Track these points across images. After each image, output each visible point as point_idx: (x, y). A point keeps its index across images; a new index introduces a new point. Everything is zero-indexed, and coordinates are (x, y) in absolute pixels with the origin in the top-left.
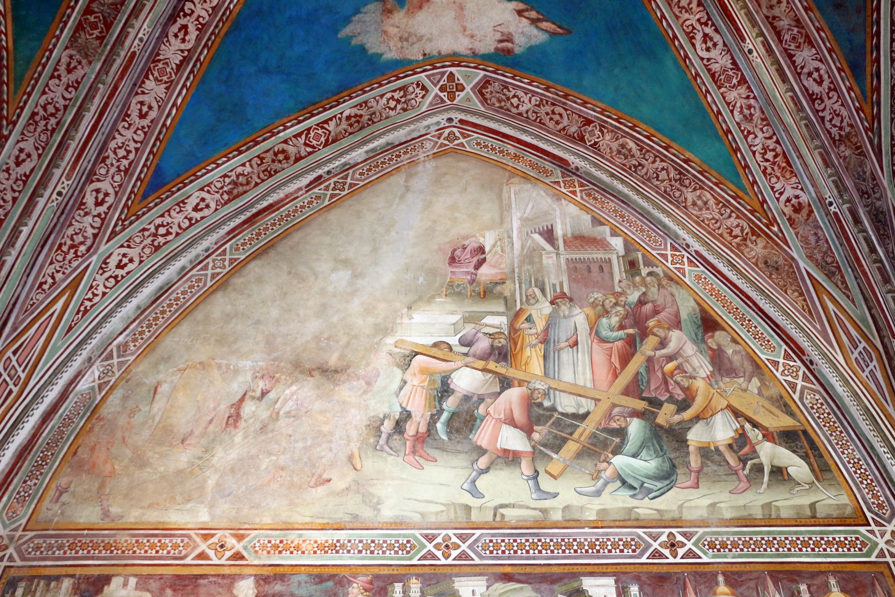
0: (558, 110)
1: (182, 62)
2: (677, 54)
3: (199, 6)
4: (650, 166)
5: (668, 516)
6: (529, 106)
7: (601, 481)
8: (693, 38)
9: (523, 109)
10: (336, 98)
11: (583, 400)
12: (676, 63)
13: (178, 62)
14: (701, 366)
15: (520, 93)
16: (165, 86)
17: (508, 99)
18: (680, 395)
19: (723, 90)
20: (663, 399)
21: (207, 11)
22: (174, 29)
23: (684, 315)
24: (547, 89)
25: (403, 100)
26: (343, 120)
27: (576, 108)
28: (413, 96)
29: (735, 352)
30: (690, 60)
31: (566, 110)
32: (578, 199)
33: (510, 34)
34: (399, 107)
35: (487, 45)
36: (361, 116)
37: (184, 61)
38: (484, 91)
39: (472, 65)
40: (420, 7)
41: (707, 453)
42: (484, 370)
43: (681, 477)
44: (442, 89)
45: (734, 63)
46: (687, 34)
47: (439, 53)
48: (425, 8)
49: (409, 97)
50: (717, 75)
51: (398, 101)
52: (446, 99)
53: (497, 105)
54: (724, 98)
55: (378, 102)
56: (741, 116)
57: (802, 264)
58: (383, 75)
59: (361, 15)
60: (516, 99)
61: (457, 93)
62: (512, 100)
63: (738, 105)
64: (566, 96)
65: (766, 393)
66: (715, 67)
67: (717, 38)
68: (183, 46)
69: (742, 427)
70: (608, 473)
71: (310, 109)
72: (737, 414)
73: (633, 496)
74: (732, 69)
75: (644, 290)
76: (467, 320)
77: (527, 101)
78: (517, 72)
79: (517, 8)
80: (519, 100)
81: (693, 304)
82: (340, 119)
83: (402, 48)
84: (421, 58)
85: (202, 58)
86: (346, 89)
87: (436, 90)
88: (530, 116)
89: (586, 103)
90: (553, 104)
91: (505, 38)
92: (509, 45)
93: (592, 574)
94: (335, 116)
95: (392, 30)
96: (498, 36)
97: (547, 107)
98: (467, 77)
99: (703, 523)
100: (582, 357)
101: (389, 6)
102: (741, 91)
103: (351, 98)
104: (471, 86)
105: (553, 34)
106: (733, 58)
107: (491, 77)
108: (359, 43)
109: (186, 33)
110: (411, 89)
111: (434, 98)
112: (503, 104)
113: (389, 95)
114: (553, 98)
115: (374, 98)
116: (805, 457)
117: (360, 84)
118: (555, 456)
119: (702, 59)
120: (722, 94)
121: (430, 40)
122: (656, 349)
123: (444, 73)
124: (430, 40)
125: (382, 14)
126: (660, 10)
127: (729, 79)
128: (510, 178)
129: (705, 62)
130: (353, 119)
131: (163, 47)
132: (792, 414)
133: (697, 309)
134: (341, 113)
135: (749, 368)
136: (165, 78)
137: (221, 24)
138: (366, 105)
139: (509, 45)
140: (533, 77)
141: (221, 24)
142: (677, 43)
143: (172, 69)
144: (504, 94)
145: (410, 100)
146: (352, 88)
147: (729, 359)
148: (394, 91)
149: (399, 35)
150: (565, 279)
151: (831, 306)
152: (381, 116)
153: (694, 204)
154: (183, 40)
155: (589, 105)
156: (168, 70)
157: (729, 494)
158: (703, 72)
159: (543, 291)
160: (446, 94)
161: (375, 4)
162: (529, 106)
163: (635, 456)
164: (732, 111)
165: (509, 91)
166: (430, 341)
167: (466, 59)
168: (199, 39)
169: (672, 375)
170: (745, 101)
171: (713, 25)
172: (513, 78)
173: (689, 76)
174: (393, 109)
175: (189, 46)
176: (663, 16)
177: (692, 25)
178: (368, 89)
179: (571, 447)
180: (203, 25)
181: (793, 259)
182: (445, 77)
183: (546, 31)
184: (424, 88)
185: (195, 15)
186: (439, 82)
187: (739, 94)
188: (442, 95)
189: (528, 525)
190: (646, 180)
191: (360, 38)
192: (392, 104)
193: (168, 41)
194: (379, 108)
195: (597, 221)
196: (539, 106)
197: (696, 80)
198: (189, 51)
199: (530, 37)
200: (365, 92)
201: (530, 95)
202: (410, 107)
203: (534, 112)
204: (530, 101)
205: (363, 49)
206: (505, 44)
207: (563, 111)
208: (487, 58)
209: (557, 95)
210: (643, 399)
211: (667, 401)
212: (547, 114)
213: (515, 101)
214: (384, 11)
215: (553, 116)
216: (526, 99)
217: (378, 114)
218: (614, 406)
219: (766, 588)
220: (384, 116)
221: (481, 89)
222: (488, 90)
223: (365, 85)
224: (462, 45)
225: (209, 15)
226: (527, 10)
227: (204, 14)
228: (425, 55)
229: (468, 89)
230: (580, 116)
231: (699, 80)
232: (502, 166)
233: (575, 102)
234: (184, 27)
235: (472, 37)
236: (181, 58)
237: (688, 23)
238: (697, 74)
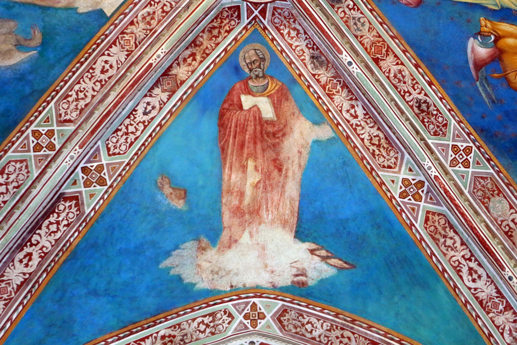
0: (347, 333)
1: (22, 283)
2: (447, 285)
3: (44, 238)
6: (321, 331)
8: (460, 271)
9: (315, 334)
10: (153, 319)
12: (447, 292)
13: (19, 283)
15: (313, 320)
16: (4, 302)
17: (303, 325)
19: (491, 315)
21: (51, 243)
22: (21, 255)
24: (337, 315)
25: (212, 324)
26: (159, 338)
27: (362, 332)
28: (221, 322)
30: (459, 289)
31: (354, 333)
33: (304, 269)
34: (208, 330)
36: (174, 337)
37: (25, 282)
38: (282, 318)
39: (272, 296)
40: (230, 247)
44: (246, 317)
45: (498, 292)
46: (455, 268)
47: (244, 286)
48: (234, 247)
49: (217, 322)
50: (484, 302)
51: (207, 326)
52: (249, 326)
53: (294, 331)
54: (493, 322)
55: (190, 325)
56: (511, 338)
58: (196, 301)
59: (180, 251)
60: (310, 325)
61: (259, 321)
62: (307, 326)
63: (507, 328)
64: (353, 321)
66: (482, 296)
67: (480, 271)
68: (25, 270)
71: (130, 327)
74: (497, 297)
77: (319, 326)
78: (310, 302)
79: (310, 248)
80: (313, 326)
82: (156, 338)
83: (213, 279)
84: (229, 289)
85: (41, 280)
86: (163, 312)
87: (241, 318)
88: (322, 340)
89: (371, 327)
90: (342, 329)
91: (300, 273)
92: (303, 278)
94: (151, 335)
95: (205, 265)
96: (294, 271)
97: (337, 331)
98: (268, 306)
101: (203, 245)
102: (507, 316)
103: (167, 320)
104: (271, 314)
105: (340, 269)
106: (497, 288)
107: (288, 307)
108: (177, 273)
109: (30, 260)
110: (219, 316)
111: (239, 325)
112: (298, 330)
113: (200, 320)
114: (342, 324)
115: (187, 321)
117: (176, 308)
119: (470, 289)
120: (491, 318)
121: (237, 274)
123: (247, 303)
124: (237, 274)
125: (197, 251)
126: (430, 248)
127: (496, 305)
129: (472, 291)
130: (167, 339)
131: (8, 270)
134: (157, 333)
136: (5, 296)
137: (61, 254)
138: (179, 327)
139: (303, 278)
140: (324, 306)
141: (61, 254)
142: (446, 275)
143: (13, 288)
144: (299, 321)
145: (217, 325)
146: (167, 311)
148: (205, 316)
149: (211, 269)
152: (192, 338)
154: (27, 265)
155: (374, 329)
156: (9, 289)
158: (472, 300)
160: (249, 321)
161: (192, 242)
162: (321, 331)
164: (502, 334)
165: (304, 318)
167: (267, 291)
168: (40, 264)
170: (513, 325)
171: (476, 260)
172: (307, 307)
173: (460, 303)
174: (202, 332)
175: (30, 270)
176: (433, 253)
177: (458, 260)
178: (182, 313)
180: (46, 254)
182: (249, 307)
183: (335, 266)
184: (230, 315)
185: (40, 246)
186: (243, 310)
187: (506, 319)
188: (245, 322)
191: (177, 269)
192: (202, 327)
193: (13, 265)
194: (190, 330)
196: (329, 330)
197: (466, 307)
198: (30, 274)
199: (321, 272)
200: (179, 316)
201: (322, 321)
202: (217, 332)
203: (325, 336)
204: (322, 326)
205: (179, 279)
206: (300, 278)
207: (350, 335)
208: (285, 290)
209: (345, 320)
212: (337, 338)
213: (309, 327)
214: (199, 248)
215: (342, 340)
216: (318, 325)
217: (189, 336)
220: (195, 338)
221: (279, 318)
222: (286, 318)
223: (180, 309)
225: (52, 246)
226: (318, 250)
227: (48, 245)
228: (232, 286)
229: (268, 317)
230: (366, 339)
231: (469, 307)
233: (361, 327)
234: (30, 255)
235: (272, 272)
236: (23, 280)
237: (454, 259)
238: (467, 302)
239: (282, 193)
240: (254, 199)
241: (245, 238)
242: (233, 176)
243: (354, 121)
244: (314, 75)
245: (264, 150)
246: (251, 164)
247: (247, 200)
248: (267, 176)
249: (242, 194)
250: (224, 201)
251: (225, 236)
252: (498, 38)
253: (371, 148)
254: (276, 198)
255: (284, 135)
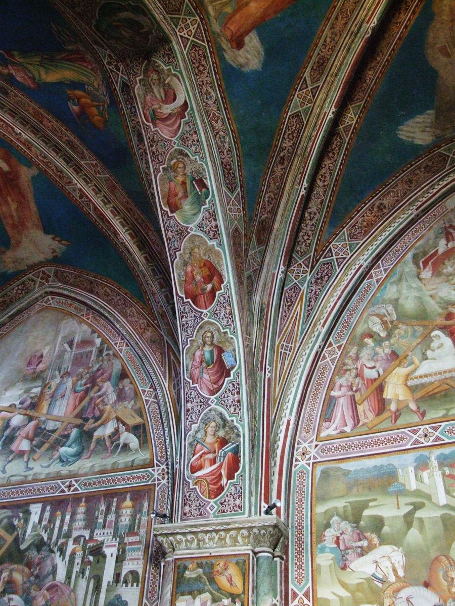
4: (116, 299)
5: (72, 473)
7: (52, 460)
11: (57, 423)
14: (112, 397)
18: (97, 413)
20: (90, 417)
23: (114, 374)
29: (130, 388)
32: (89, 321)
34: (23, 292)
35: (50, 256)
36: (5, 301)
40: (18, 246)
41: (100, 441)
42: (25, 415)
43: (85, 455)
57: (165, 337)
65: (134, 408)
69: (118, 426)
70: (56, 456)
72: (118, 419)
73: (62, 466)
75: (101, 363)
76: (25, 392)
81: (120, 367)
87: (39, 280)
93: (34, 503)
95: (8, 260)
99: (86, 475)
100: (65, 402)
113: (16, 288)
116: (139, 438)
118: (38, 451)
121: (27, 259)
122: (96, 393)
123: (39, 272)
128: (65, 316)
132: (141, 416)
133: (121, 368)
135: (132, 395)
147: (125, 393)
150: (70, 365)
151: (172, 357)
153: (130, 315)
157: (100, 460)
159: (60, 372)
163: (69, 447)
166: (8, 404)
169: (98, 404)
174: (20, 294)
179: (47, 445)
181: (162, 336)
184: (33, 281)
188: (42, 281)
189: (17, 483)
190: (115, 307)
192: (19, 292)
195: (94, 332)
210: (82, 418)
211: (92, 418)
218: (69, 423)
219: (100, 502)
224: (40, 258)
229: (52, 276)
232: (62, 311)
239: (30, 210)
240: (19, 217)
241: (24, 239)
242: (3, 209)
243: (45, 160)
244: (18, 139)
245: (13, 189)
246: (9, 199)
247: (16, 219)
248: (20, 203)
249: (12, 217)
250: (4, 223)
251: (13, 241)
252: (78, 99)
253: (58, 174)
254: (29, 214)
255: (18, 177)
